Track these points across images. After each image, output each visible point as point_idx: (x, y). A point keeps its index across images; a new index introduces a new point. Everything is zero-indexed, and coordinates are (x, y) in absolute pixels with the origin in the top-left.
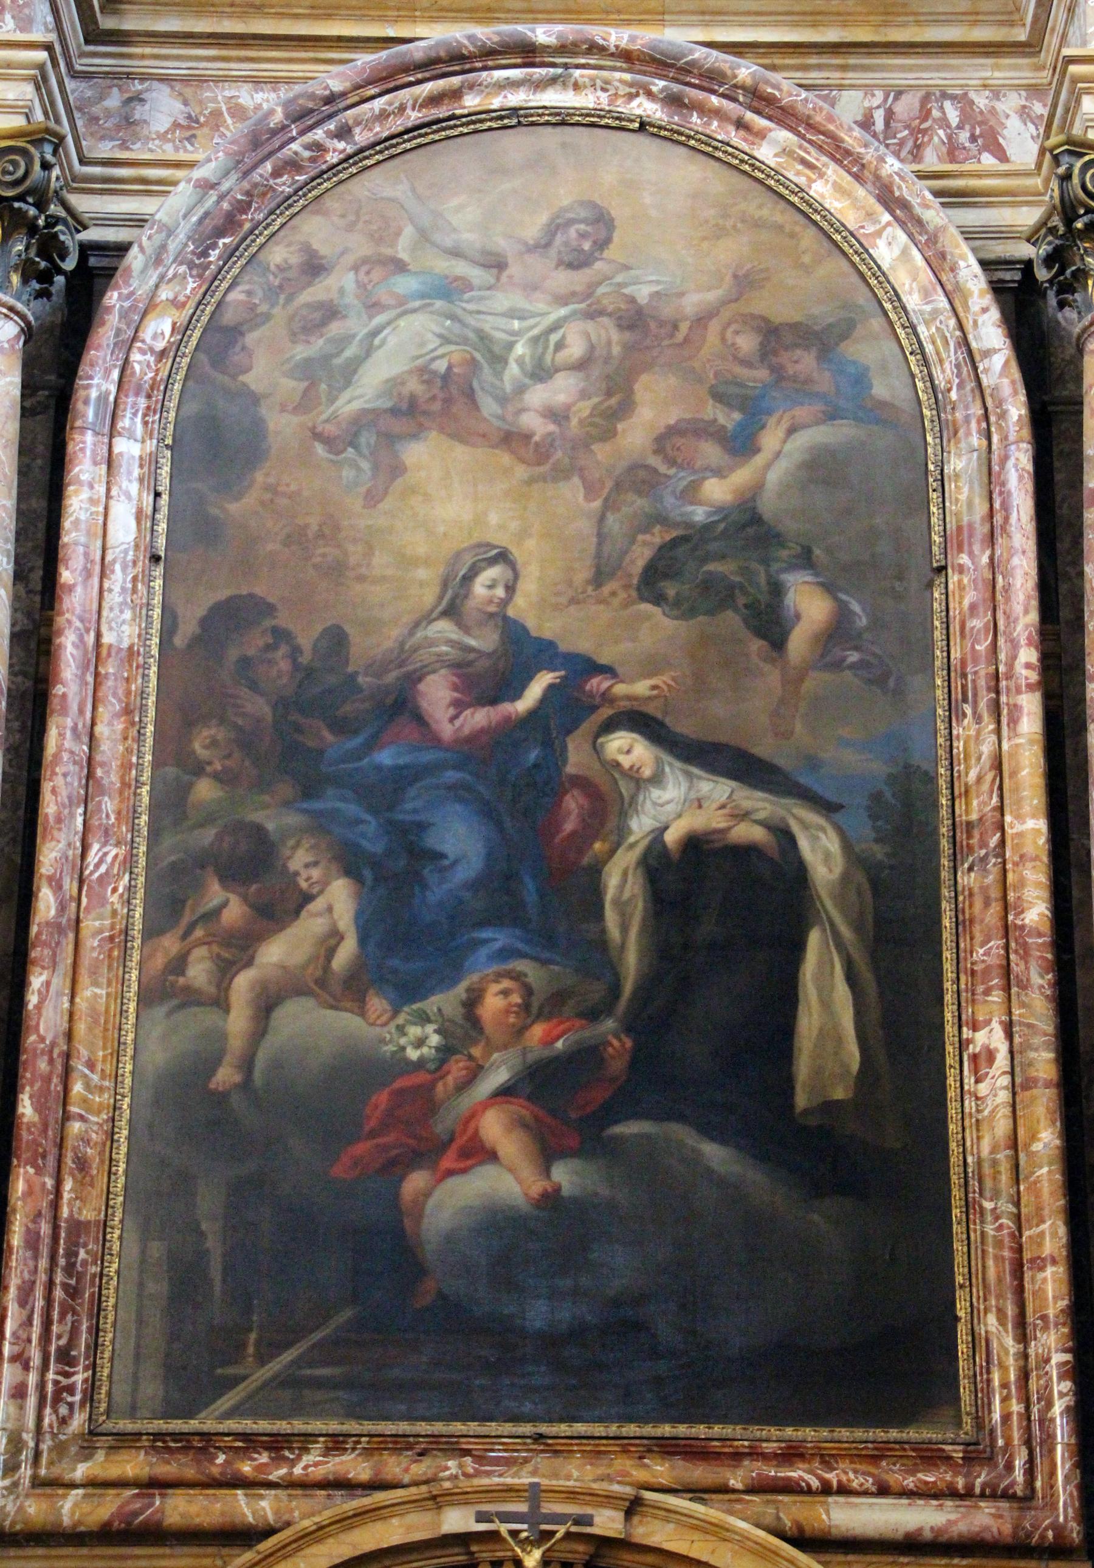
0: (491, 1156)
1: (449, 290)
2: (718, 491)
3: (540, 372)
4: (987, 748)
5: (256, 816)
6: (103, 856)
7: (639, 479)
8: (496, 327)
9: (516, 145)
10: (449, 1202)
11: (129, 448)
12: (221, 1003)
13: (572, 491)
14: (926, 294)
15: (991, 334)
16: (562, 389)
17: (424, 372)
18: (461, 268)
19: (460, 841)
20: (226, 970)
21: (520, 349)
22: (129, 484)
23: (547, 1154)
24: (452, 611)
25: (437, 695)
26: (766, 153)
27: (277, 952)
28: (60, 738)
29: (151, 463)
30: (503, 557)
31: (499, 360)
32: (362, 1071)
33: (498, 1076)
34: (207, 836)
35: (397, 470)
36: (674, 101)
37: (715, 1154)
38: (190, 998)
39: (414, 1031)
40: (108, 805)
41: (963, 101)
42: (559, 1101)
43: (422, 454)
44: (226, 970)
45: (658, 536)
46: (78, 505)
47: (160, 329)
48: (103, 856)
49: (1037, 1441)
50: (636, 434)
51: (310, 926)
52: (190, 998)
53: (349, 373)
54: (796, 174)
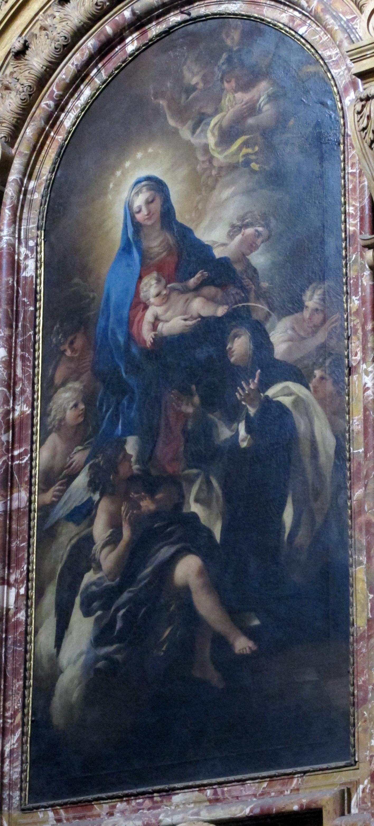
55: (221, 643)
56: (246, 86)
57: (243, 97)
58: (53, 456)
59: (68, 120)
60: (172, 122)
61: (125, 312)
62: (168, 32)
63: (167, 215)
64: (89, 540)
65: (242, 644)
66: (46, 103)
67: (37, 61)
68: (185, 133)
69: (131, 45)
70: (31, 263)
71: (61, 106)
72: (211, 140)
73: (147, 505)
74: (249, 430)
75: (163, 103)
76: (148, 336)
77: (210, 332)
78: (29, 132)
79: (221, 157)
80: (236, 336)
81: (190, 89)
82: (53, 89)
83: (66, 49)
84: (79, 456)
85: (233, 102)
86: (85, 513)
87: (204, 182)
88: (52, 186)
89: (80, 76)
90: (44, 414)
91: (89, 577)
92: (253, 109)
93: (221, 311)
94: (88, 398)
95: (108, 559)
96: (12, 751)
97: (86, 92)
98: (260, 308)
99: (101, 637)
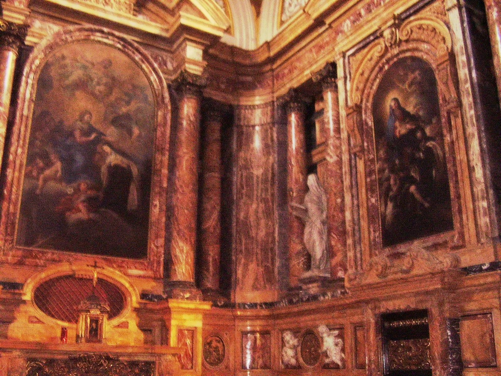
0: (80, 211)
1: (85, 68)
2: (124, 110)
3: (98, 84)
4: (160, 159)
5: (47, 149)
6: (20, 151)
7: (112, 105)
8: (93, 76)
9: (98, 46)
10: (73, 217)
11: (30, 81)
12: (38, 179)
13: (101, 105)
14: (158, 86)
15: (167, 95)
16: (102, 88)
17: (80, 79)
18: (87, 64)
19: (80, 159)
20: (39, 174)
21: (96, 80)
22: (29, 87)
23: (89, 210)
24: (81, 121)
25: (77, 134)
26: (137, 58)
27: (48, 172)
28: (15, 129)
29: (33, 84)
30: (90, 114)
31: (92, 80)
32: (62, 194)
33: (83, 198)
34: (37, 150)
35: (74, 95)
36: (123, 46)
37: (115, 215)
38: (33, 178)
39: (69, 189)
40: (21, 142)
41: (162, 58)
42: (92, 203)
43: (78, 93)
44: (39, 174)
45: (114, 115)
46: (22, 89)
47: (37, 62)
48: (20, 151)
49: (159, 262)
50: (112, 98)
51: (53, 169)
52: (33, 178)
53: (68, 77)
54: (140, 62)
55: (422, 205)
57: (412, 75)
58: (380, 166)
64: (390, 185)
65: (427, 205)
67: (366, 75)
68: (401, 86)
71: (372, 84)
72: (406, 86)
73: (402, 175)
74: (423, 154)
76: (397, 134)
77: (412, 132)
84: (386, 166)
85: (411, 77)
86: (388, 179)
87: (406, 98)
91: (391, 194)
92: (415, 78)
93: (414, 127)
94: (386, 152)
95: (395, 189)
98: (422, 124)
99: (395, 207)
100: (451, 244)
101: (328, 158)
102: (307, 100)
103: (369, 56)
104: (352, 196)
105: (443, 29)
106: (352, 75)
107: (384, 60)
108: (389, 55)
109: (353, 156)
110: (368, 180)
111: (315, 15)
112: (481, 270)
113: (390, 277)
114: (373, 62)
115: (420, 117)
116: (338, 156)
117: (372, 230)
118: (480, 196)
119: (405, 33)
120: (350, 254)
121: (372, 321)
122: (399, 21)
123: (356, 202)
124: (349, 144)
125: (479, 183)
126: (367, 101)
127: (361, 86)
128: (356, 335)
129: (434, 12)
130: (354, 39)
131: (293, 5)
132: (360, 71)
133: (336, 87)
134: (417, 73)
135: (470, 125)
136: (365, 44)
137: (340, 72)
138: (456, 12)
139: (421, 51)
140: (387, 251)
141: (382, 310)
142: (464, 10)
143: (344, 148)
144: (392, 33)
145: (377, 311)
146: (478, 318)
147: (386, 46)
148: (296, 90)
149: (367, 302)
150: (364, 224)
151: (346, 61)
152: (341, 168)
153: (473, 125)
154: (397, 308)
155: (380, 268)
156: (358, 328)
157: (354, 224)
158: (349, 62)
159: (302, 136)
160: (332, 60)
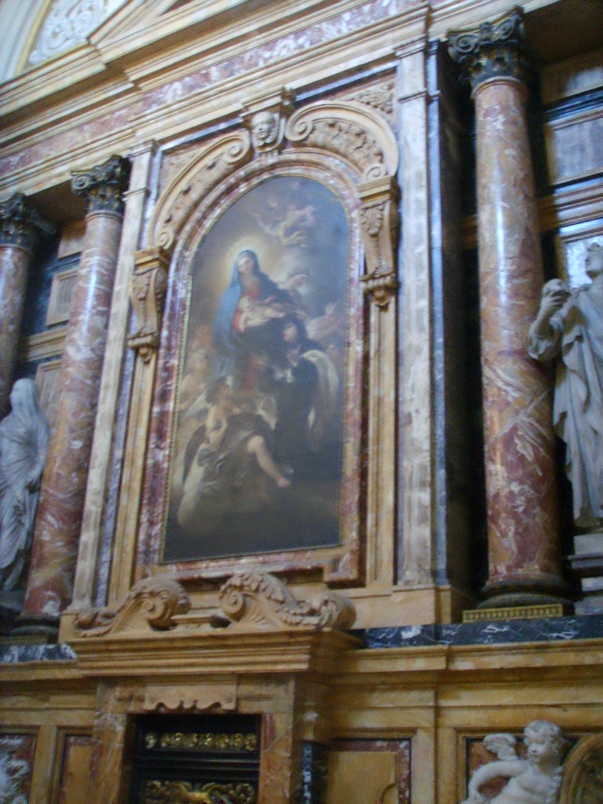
55: (272, 481)
56: (300, 208)
57: (299, 213)
59: (208, 224)
60: (261, 224)
61: (231, 315)
62: (262, 183)
63: (255, 268)
66: (197, 215)
67: (194, 195)
68: (267, 229)
69: (243, 188)
70: (184, 291)
71: (204, 217)
72: (280, 232)
74: (293, 374)
75: (257, 215)
76: (241, 327)
77: (275, 326)
78: (188, 228)
79: (285, 241)
80: (289, 327)
81: (272, 209)
82: (202, 207)
83: (210, 190)
84: (202, 386)
85: (293, 215)
86: (204, 413)
88: (197, 255)
89: (215, 203)
90: (185, 366)
91: (203, 446)
92: (303, 219)
93: (281, 315)
95: (214, 436)
96: (156, 534)
97: (218, 211)
98: (301, 314)
99: (207, 477)
100: (328, 577)
101: (71, 351)
102: (46, 227)
103: (208, 161)
104: (113, 439)
105: (381, 135)
106: (164, 192)
107: (241, 173)
108: (254, 165)
109: (130, 354)
110: (156, 409)
111: (109, 56)
112: (397, 640)
113: (179, 631)
114: (215, 173)
115: (298, 296)
116: (93, 350)
117: (144, 518)
118: (416, 478)
119: (299, 128)
120: (85, 567)
121: (120, 729)
122: (291, 103)
123: (118, 454)
124: (128, 329)
125: (419, 450)
126: (186, 247)
127: (179, 215)
128: (65, 756)
129: (368, 103)
130: (185, 121)
131: (61, 38)
132: (183, 186)
133: (122, 209)
134: (308, 210)
135: (414, 328)
136: (204, 136)
137: (138, 180)
138: (419, 105)
139: (328, 169)
140: (173, 572)
141: (149, 706)
142: (434, 106)
143: (116, 333)
144: (272, 122)
145: (133, 708)
146: (377, 749)
147: (252, 150)
148: (29, 201)
149: (111, 681)
150: (130, 504)
151: (157, 160)
152: (97, 377)
153: (421, 330)
154: (187, 706)
155: (159, 604)
156: (72, 739)
157: (106, 499)
158: (161, 167)
159: (18, 299)
160: (124, 155)
